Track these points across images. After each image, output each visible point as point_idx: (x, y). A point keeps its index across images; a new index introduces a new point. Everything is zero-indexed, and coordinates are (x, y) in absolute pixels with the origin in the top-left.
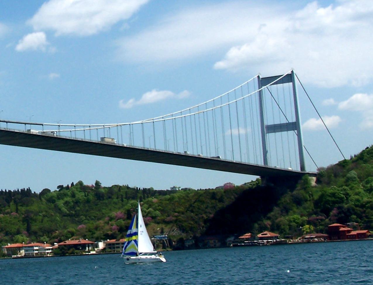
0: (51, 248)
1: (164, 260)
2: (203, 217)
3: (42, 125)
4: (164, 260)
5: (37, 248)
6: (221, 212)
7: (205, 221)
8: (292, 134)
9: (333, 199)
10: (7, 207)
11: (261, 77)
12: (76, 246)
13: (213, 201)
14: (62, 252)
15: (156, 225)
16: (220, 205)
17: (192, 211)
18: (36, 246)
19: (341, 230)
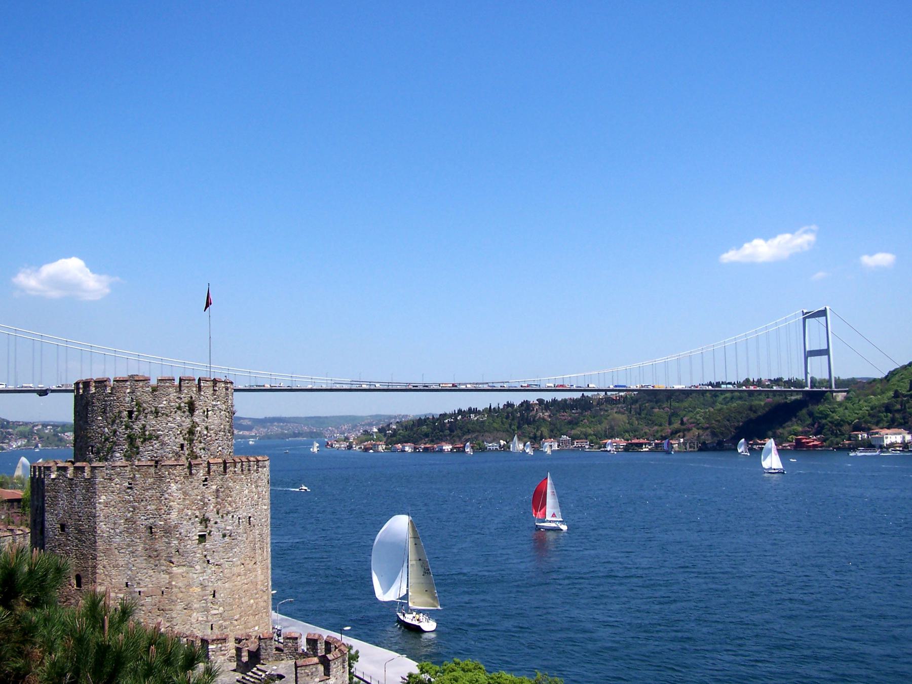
1: (749, 454)
4: (749, 454)
5: (615, 444)
7: (736, 428)
9: (820, 415)
11: (805, 311)
13: (749, 412)
16: (753, 416)
17: (728, 420)
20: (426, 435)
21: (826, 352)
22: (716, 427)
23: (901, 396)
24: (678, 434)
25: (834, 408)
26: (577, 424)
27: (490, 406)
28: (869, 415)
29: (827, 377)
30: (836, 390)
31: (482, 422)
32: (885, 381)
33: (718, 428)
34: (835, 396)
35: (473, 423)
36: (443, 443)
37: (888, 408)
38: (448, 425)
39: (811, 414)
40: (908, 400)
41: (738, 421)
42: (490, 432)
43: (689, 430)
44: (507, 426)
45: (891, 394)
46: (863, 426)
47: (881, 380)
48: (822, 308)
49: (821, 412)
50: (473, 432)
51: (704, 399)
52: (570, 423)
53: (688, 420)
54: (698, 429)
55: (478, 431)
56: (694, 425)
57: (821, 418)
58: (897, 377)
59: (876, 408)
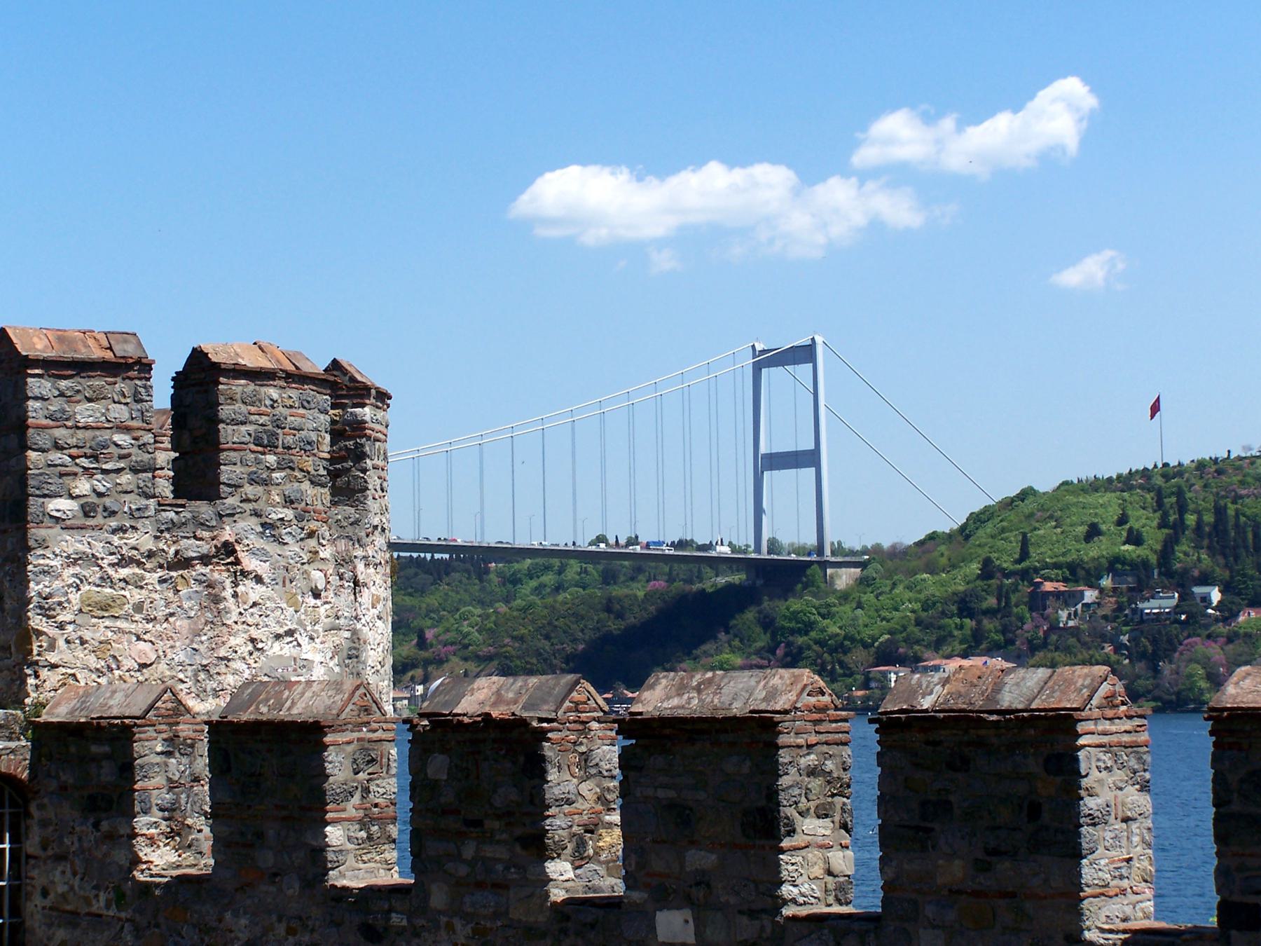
6: (607, 639)
9: (793, 625)
11: (759, 347)
13: (604, 615)
16: (614, 626)
17: (547, 637)
21: (809, 458)
22: (513, 653)
23: (998, 575)
24: (410, 674)
25: (828, 605)
28: (918, 623)
29: (811, 446)
30: (833, 559)
32: (961, 538)
33: (519, 657)
34: (832, 577)
37: (965, 606)
39: (767, 623)
40: (1016, 585)
41: (574, 640)
43: (440, 662)
45: (975, 567)
46: (901, 650)
47: (949, 537)
48: (805, 341)
49: (794, 616)
51: (483, 589)
53: (436, 637)
54: (466, 659)
56: (452, 648)
57: (792, 632)
58: (989, 528)
59: (934, 604)
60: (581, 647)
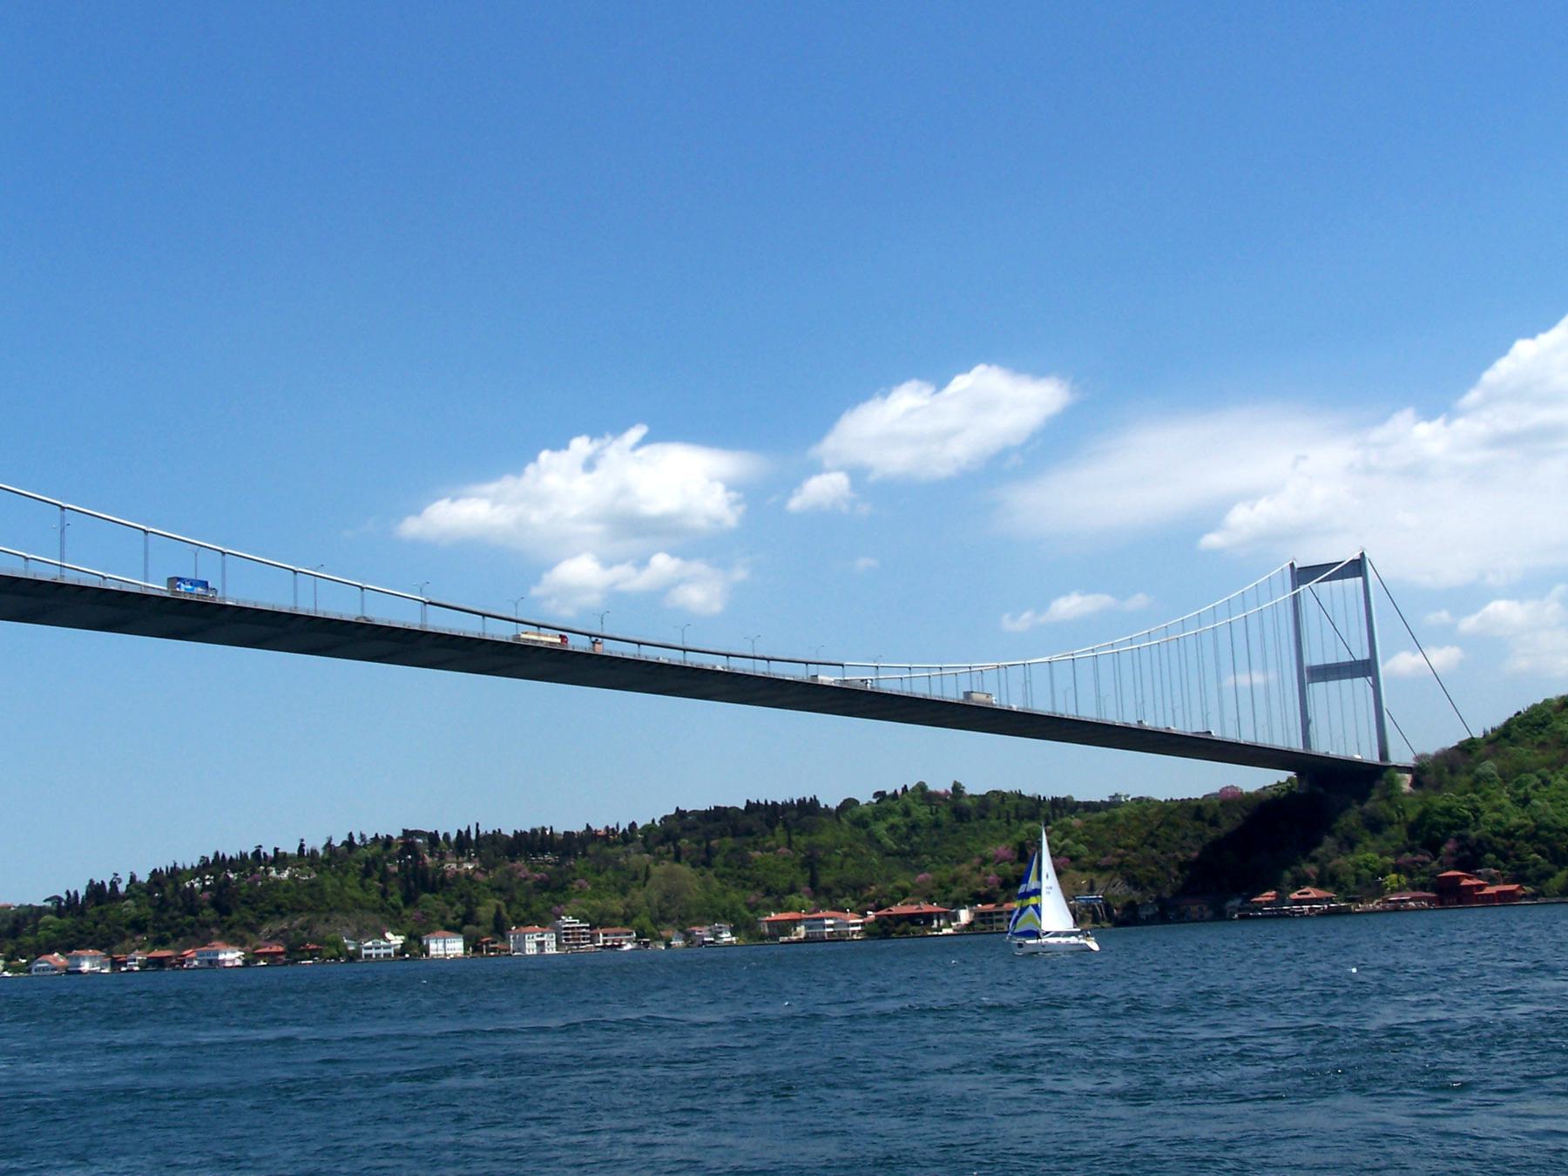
0: (861, 921)
1: (1095, 946)
2: (1176, 858)
3: (843, 665)
4: (1095, 946)
6: (1217, 846)
7: (1182, 867)
8: (1362, 684)
9: (1447, 820)
10: (769, 837)
11: (1297, 566)
12: (912, 918)
13: (1198, 824)
14: (883, 930)
15: (1080, 874)
16: (1212, 833)
17: (1154, 845)
18: (828, 918)
19: (1463, 884)
20: (138, 926)
26: (562, 888)
27: (302, 846)
31: (312, 885)
35: (287, 889)
36: (217, 945)
38: (206, 895)
42: (347, 912)
44: (375, 896)
48: (1356, 556)
50: (297, 909)
52: (543, 886)
54: (1083, 870)
55: (310, 910)
60: (1195, 854)
